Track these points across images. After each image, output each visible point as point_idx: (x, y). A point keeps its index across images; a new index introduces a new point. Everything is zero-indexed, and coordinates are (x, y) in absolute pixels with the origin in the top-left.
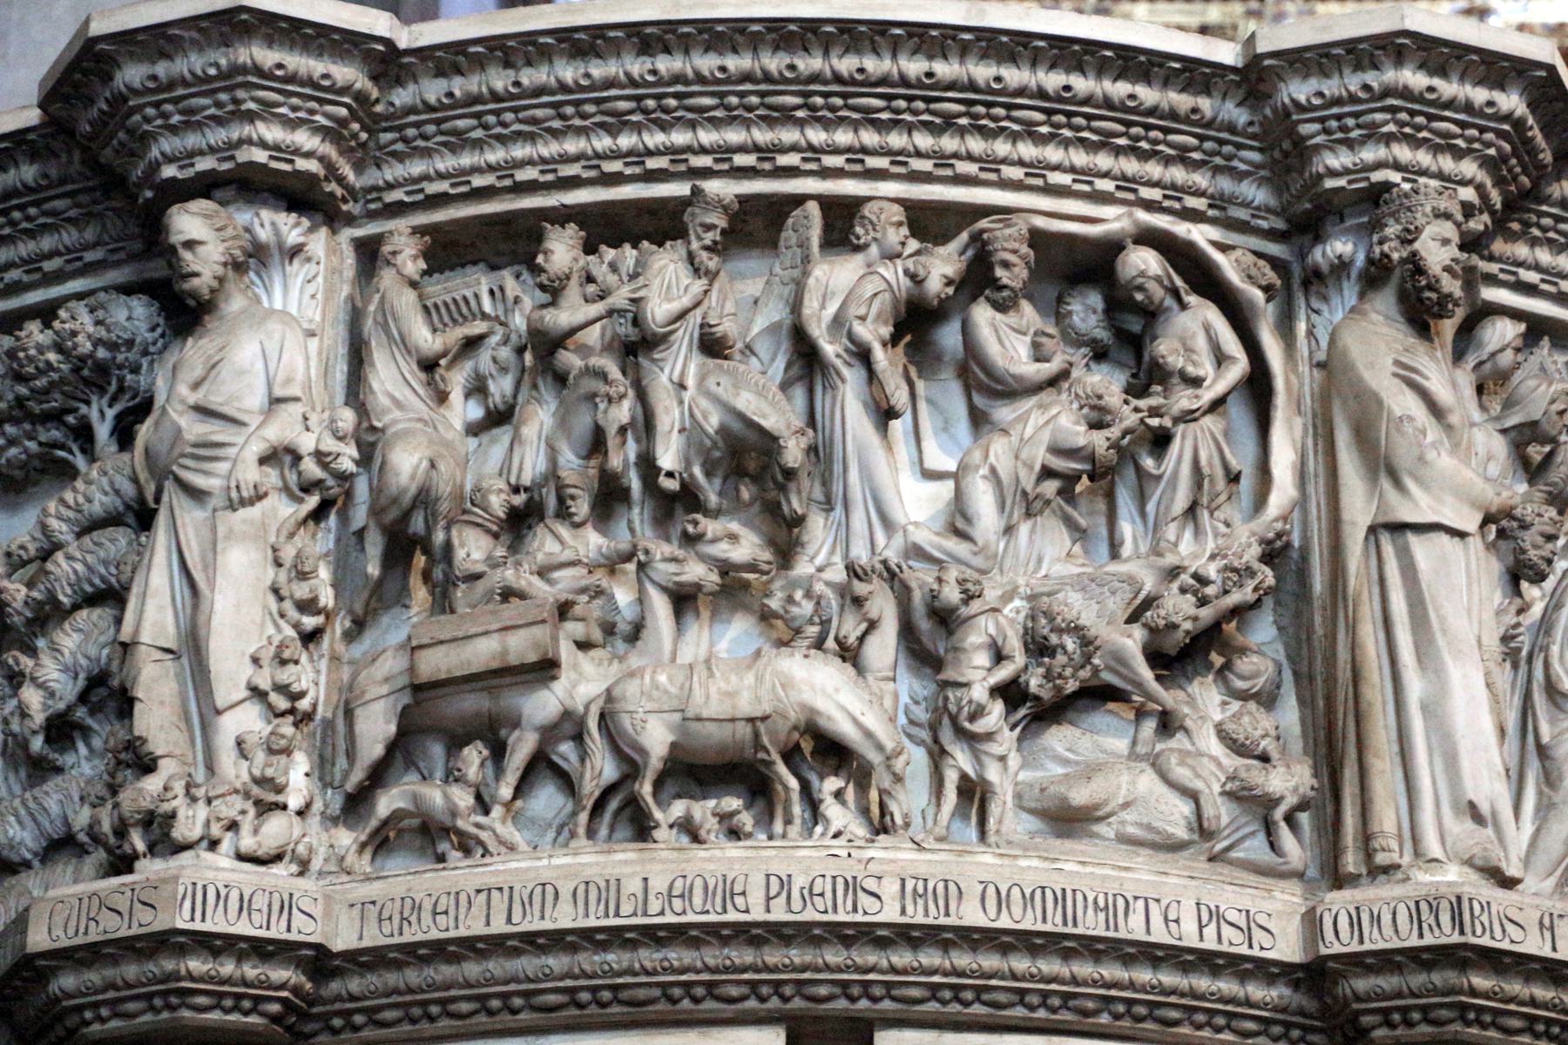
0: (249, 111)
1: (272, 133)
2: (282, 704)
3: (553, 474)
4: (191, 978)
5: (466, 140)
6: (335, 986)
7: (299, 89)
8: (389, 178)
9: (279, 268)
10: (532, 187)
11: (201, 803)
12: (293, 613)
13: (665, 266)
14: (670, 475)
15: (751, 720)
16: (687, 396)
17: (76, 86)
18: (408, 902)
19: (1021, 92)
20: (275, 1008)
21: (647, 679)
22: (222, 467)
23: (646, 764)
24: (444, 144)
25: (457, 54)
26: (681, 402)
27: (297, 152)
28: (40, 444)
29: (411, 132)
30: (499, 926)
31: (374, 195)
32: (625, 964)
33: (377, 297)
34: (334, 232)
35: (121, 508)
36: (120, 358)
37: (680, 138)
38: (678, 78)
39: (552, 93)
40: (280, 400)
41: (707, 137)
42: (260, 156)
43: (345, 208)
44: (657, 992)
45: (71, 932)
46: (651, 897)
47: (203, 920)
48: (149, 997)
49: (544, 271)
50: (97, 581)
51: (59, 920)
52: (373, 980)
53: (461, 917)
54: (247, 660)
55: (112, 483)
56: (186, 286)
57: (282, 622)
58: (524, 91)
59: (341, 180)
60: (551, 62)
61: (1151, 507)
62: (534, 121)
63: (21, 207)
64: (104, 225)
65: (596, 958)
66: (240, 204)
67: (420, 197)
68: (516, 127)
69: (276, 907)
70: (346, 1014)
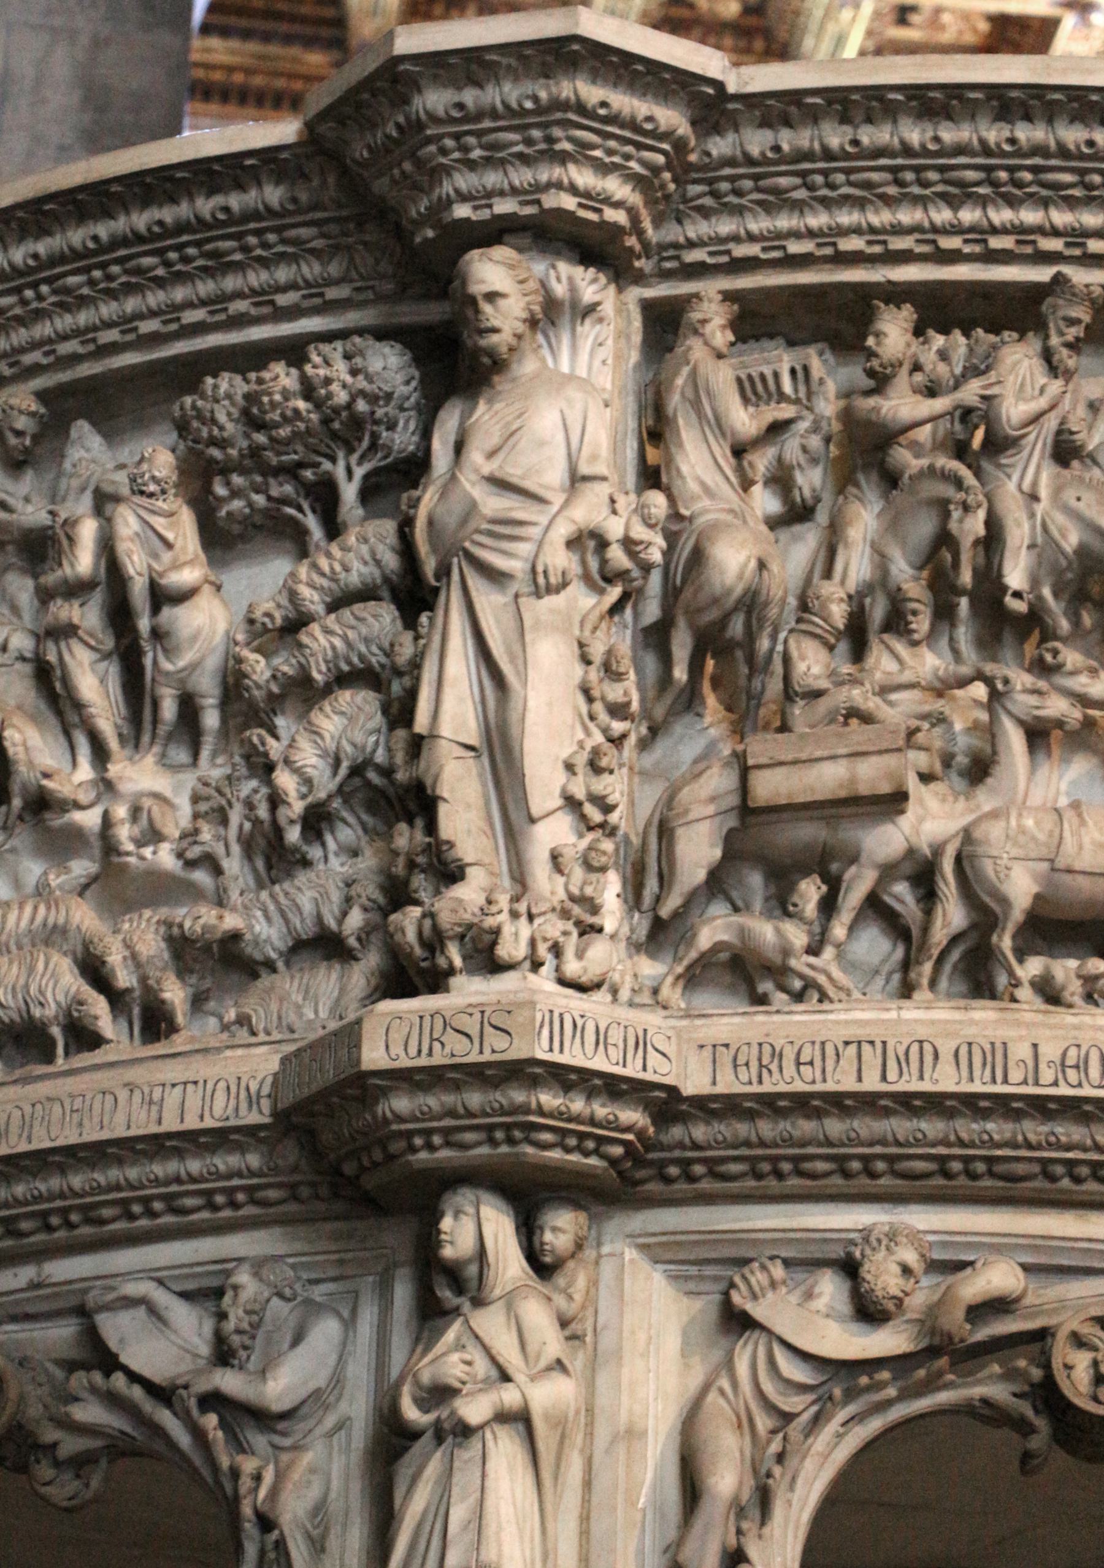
0: (564, 151)
2: (596, 816)
3: (882, 581)
4: (541, 1112)
5: (785, 200)
6: (677, 1132)
7: (618, 131)
8: (692, 234)
9: (568, 326)
10: (855, 259)
11: (524, 920)
12: (603, 717)
13: (1019, 362)
14: (1017, 595)
16: (1040, 509)
17: (359, 106)
18: (767, 1049)
20: (617, 1151)
21: (1013, 822)
22: (525, 549)
23: (1006, 917)
24: (760, 203)
25: (789, 104)
26: (1032, 515)
27: (608, 201)
29: (725, 186)
30: (871, 1083)
31: (671, 252)
32: (1008, 1135)
33: (686, 370)
34: (620, 290)
35: (379, 581)
36: (380, 413)
37: (1030, 216)
38: (1039, 150)
39: (893, 155)
40: (586, 479)
41: (1061, 218)
42: (569, 202)
43: (637, 264)
44: (1036, 1168)
46: (1043, 1066)
47: (561, 1051)
48: (490, 1128)
49: (876, 355)
50: (355, 660)
51: (397, 1037)
52: (724, 1129)
53: (829, 1068)
54: (560, 767)
55: (373, 553)
56: (484, 342)
57: (591, 726)
58: (862, 150)
59: (640, 233)
60: (895, 122)
62: (868, 185)
63: (258, 233)
64: (352, 260)
65: (974, 1126)
66: (533, 253)
67: (725, 259)
69: (631, 1042)
70: (685, 1164)
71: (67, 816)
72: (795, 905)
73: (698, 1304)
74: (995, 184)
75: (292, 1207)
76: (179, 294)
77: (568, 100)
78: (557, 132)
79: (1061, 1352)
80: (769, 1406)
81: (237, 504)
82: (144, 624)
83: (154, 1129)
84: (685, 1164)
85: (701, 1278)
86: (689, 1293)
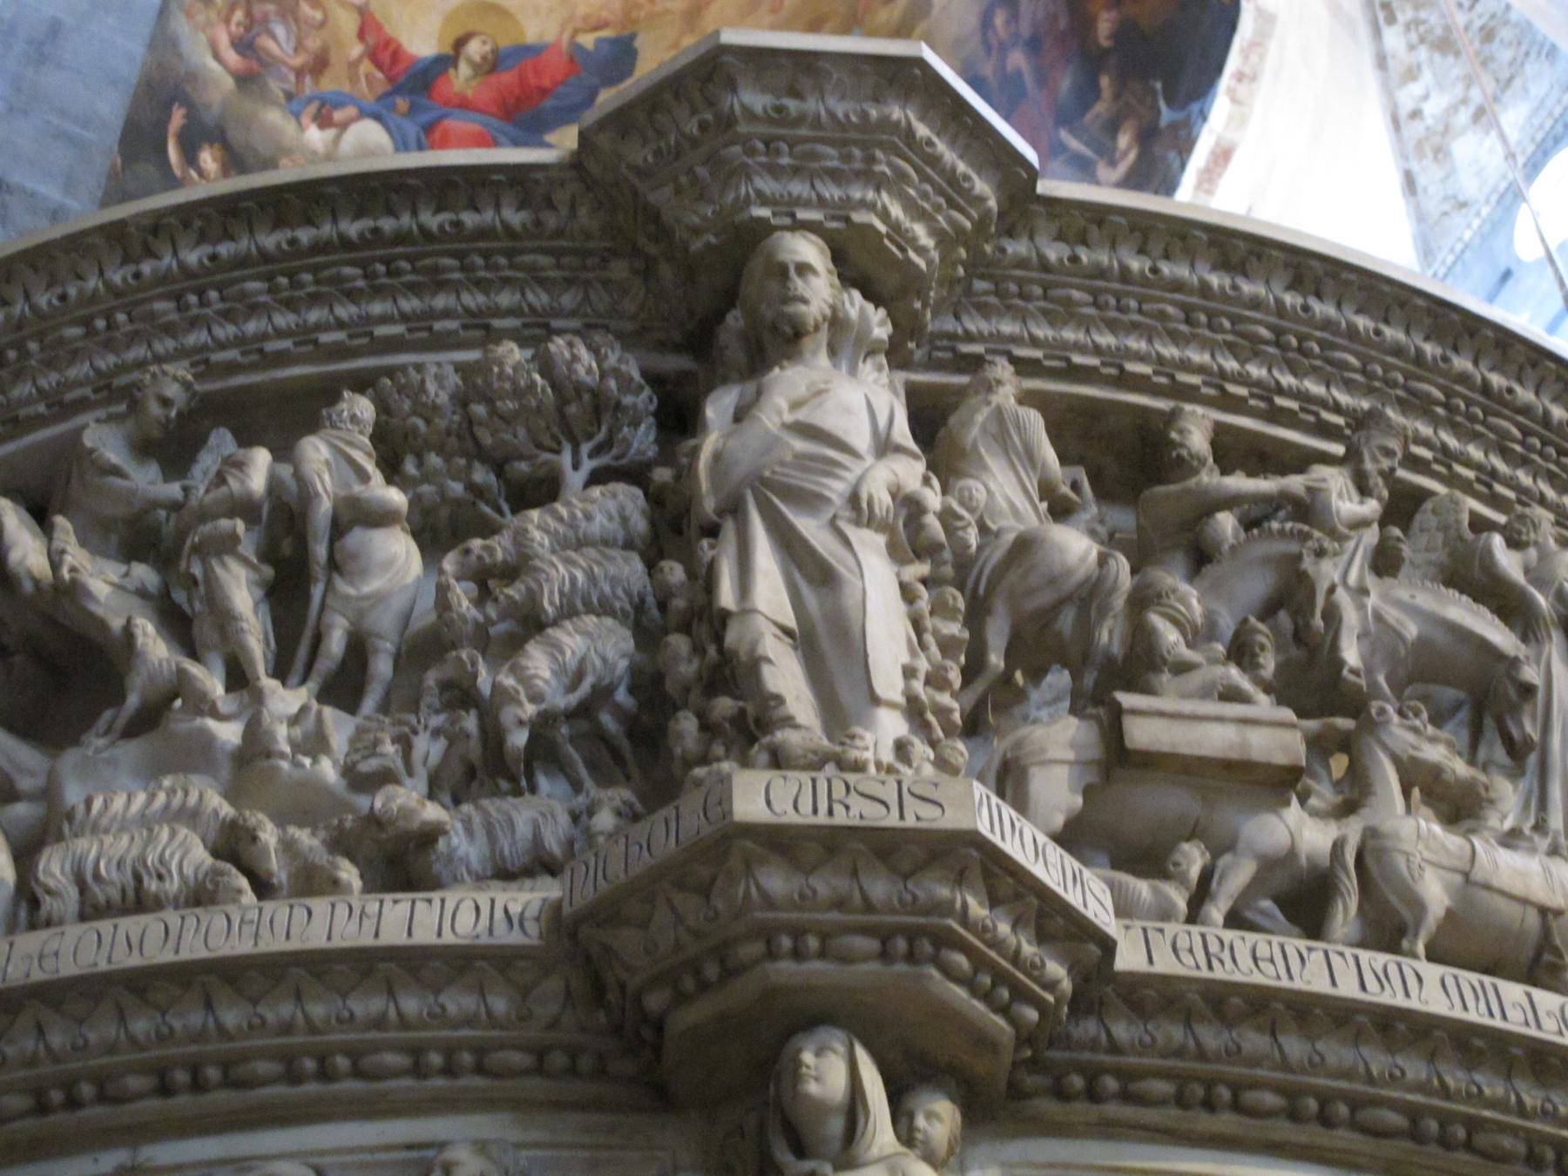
1: (896, 211)
7: (936, 177)
8: (972, 327)
14: (1354, 672)
15: (1544, 911)
16: (1372, 601)
26: (1361, 607)
27: (913, 241)
28: (471, 487)
36: (628, 400)
37: (1314, 388)
38: (1327, 324)
45: (806, 804)
49: (1182, 445)
56: (792, 309)
64: (587, 297)
68: (1136, 317)
71: (199, 721)
72: (1176, 864)
75: (535, 1086)
76: (377, 308)
77: (898, 122)
78: (879, 154)
82: (320, 551)
83: (367, 940)
84: (1092, 1074)
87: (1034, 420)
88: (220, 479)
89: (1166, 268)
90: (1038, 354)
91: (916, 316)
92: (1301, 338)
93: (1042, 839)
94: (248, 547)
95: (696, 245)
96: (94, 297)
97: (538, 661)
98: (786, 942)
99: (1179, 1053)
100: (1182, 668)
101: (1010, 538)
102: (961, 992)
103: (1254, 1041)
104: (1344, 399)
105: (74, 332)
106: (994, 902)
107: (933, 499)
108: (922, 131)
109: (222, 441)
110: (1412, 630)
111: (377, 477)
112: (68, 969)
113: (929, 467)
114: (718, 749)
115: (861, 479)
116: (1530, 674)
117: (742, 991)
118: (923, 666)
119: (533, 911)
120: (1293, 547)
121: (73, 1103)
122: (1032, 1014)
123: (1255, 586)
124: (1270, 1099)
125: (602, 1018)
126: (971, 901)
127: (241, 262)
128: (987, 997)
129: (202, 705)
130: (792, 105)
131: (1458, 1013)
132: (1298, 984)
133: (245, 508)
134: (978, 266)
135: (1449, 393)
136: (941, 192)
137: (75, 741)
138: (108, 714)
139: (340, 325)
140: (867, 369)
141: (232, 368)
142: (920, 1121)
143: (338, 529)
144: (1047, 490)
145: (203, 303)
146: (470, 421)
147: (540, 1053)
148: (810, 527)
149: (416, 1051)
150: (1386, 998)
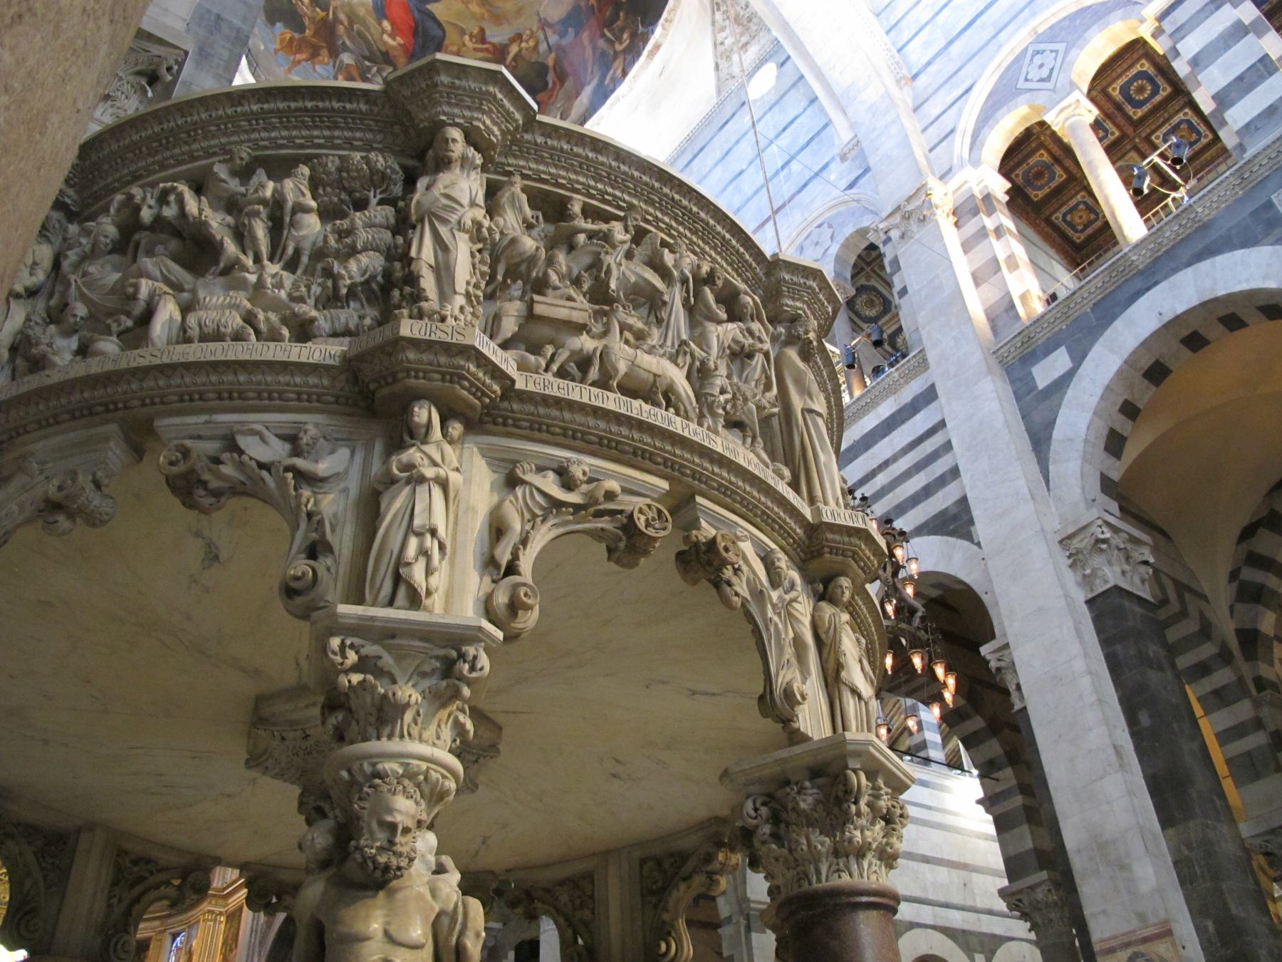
1: (488, 122)
15: (655, 375)
16: (622, 268)
19: (718, 233)
26: (619, 270)
27: (493, 133)
28: (340, 199)
36: (394, 176)
37: (618, 193)
38: (625, 173)
45: (422, 333)
61: (744, 375)
62: (572, 165)
71: (243, 274)
73: (496, 476)
74: (610, 179)
75: (335, 406)
76: (316, 133)
79: (636, 515)
80: (530, 510)
81: (325, 198)
82: (287, 219)
83: (285, 359)
84: (505, 418)
85: (499, 466)
86: (493, 471)
87: (524, 197)
88: (256, 191)
89: (575, 149)
90: (530, 173)
91: (493, 157)
92: (616, 177)
93: (496, 347)
94: (264, 215)
95: (421, 126)
96: (221, 117)
97: (353, 266)
98: (413, 374)
99: (532, 414)
100: (556, 288)
101: (510, 237)
102: (466, 393)
103: (555, 413)
104: (627, 198)
105: (213, 128)
106: (478, 366)
107: (486, 223)
108: (500, 96)
109: (261, 175)
110: (633, 279)
111: (308, 195)
112: (191, 359)
113: (487, 212)
114: (404, 304)
115: (463, 215)
116: (666, 298)
117: (397, 388)
118: (474, 280)
119: (338, 354)
120: (599, 249)
121: (192, 400)
122: (487, 400)
123: (586, 260)
124: (558, 430)
125: (357, 389)
126: (471, 366)
127: (271, 111)
128: (474, 395)
129: (244, 268)
130: (457, 82)
131: (618, 410)
132: (570, 397)
133: (263, 202)
134: (514, 141)
135: (661, 200)
136: (503, 116)
137: (203, 276)
138: (214, 268)
139: (303, 137)
140: (473, 175)
141: (266, 148)
142: (450, 430)
143: (294, 212)
144: (525, 221)
145: (257, 124)
146: (341, 178)
147: (337, 398)
148: (443, 231)
149: (299, 394)
150: (596, 404)
